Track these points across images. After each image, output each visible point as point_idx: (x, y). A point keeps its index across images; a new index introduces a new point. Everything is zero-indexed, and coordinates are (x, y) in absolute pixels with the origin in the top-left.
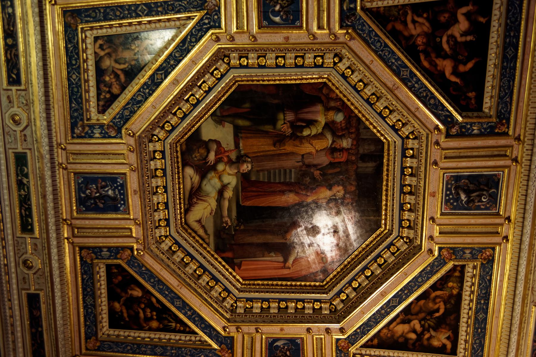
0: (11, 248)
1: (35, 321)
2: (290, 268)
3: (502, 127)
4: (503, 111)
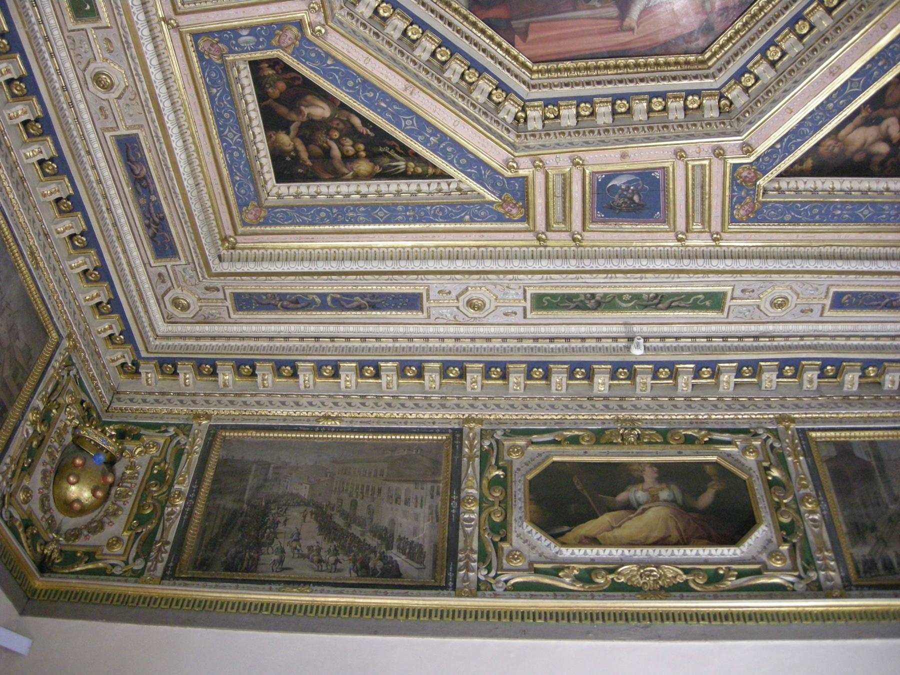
0: (64, 54)
1: (141, 184)
2: (632, 29)
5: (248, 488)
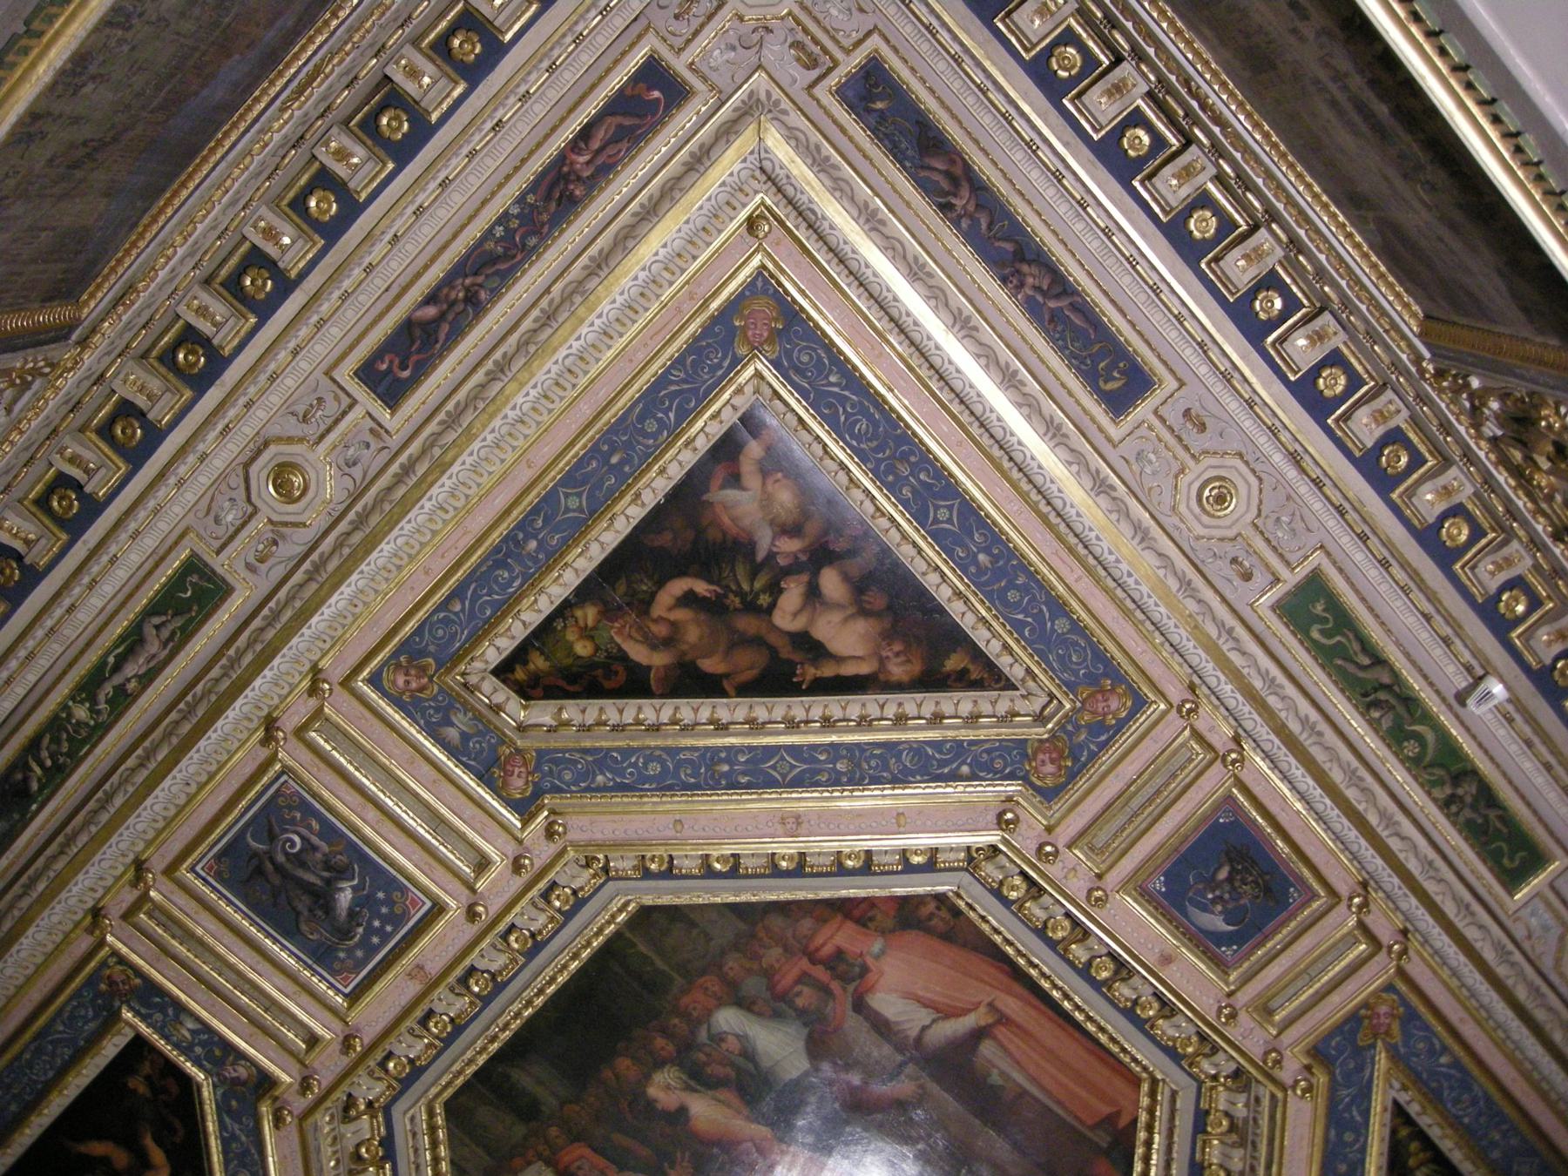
2: (991, 1005)
3: (119, 978)
4: (91, 1013)
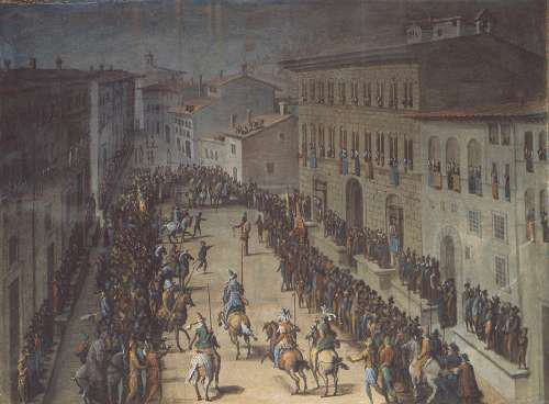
5: (94, 157)
